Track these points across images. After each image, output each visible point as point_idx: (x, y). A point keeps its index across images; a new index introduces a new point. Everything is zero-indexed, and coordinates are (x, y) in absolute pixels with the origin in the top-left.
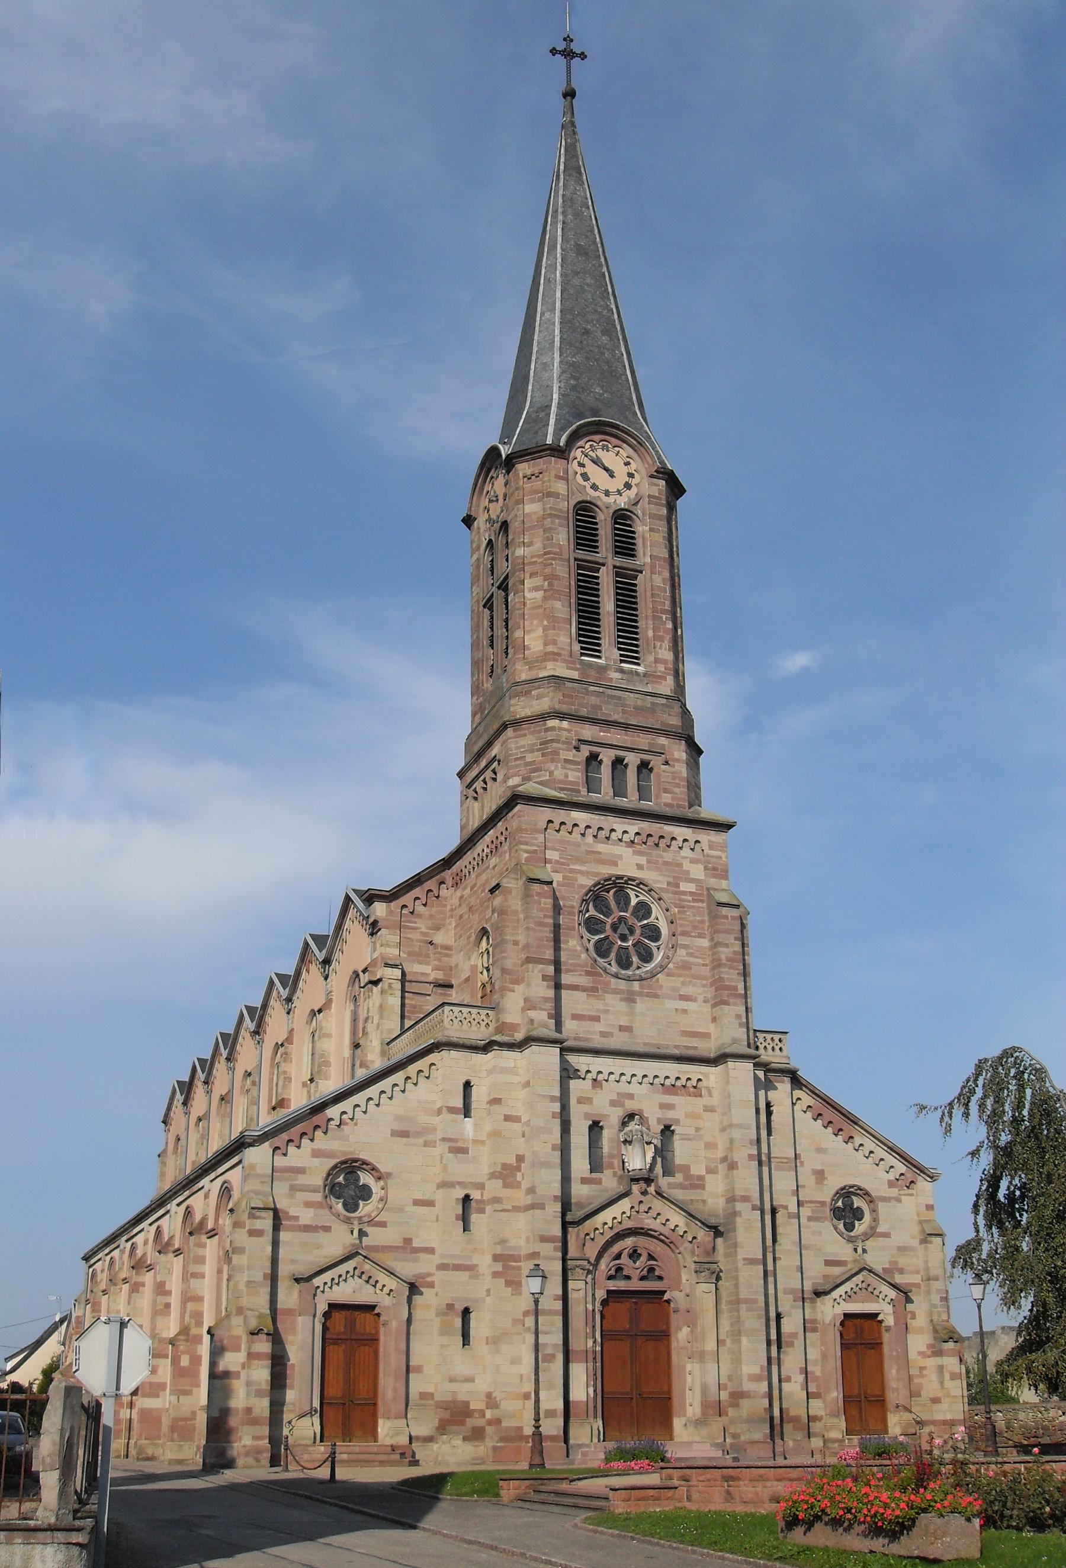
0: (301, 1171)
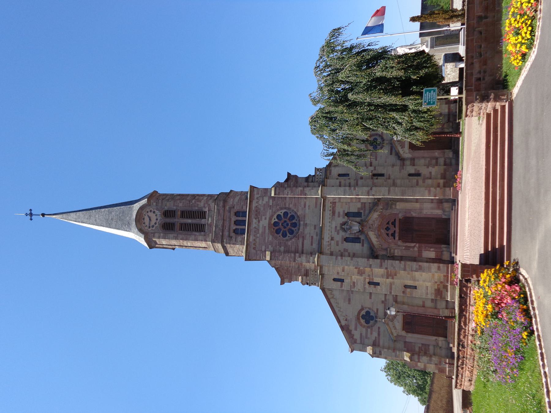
0: (361, 334)
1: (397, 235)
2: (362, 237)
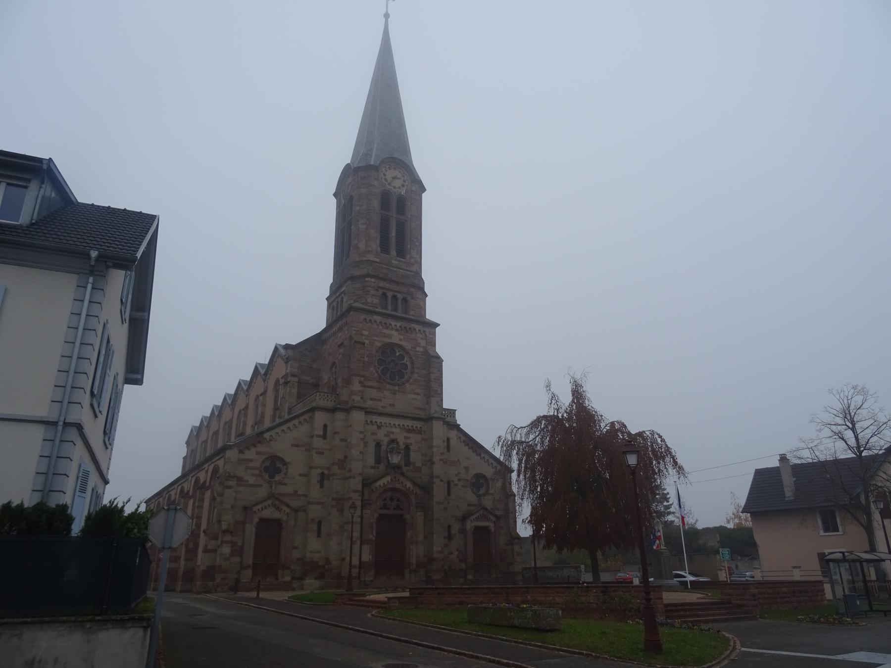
0: (251, 460)
1: (385, 512)
2: (382, 467)
